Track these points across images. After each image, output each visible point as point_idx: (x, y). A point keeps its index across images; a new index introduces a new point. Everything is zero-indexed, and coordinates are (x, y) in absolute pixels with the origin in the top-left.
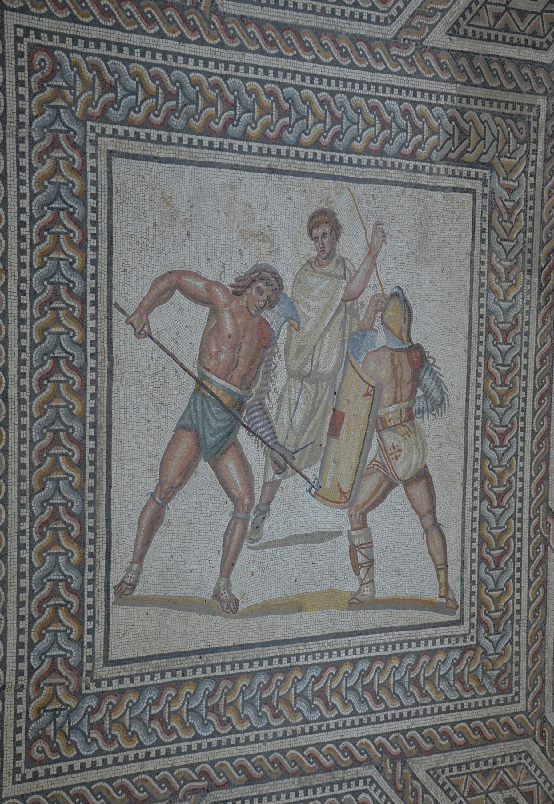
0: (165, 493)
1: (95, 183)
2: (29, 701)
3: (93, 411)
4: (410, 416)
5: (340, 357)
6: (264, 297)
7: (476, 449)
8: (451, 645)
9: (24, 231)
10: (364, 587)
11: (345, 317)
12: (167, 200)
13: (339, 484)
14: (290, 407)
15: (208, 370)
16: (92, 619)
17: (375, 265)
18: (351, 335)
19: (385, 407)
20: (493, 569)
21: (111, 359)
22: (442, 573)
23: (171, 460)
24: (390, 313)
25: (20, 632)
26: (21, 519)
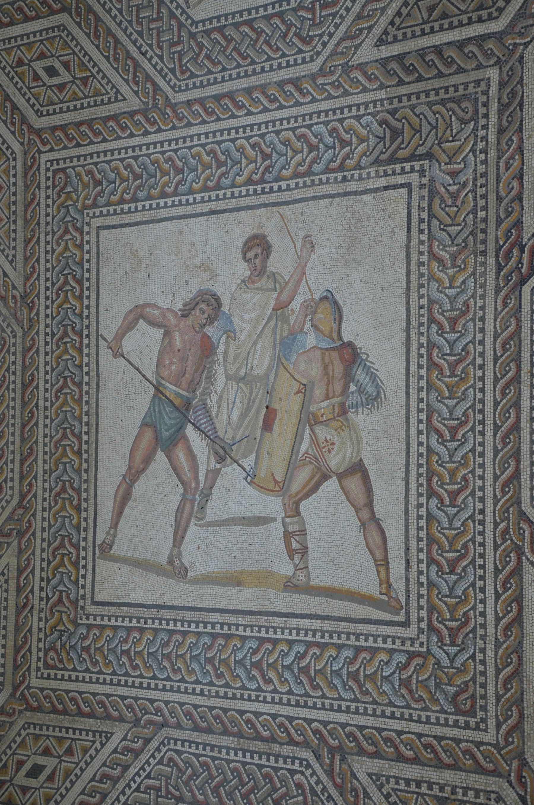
1: (88, 252)
2: (47, 621)
4: (344, 411)
5: (272, 359)
6: (206, 316)
7: (420, 444)
8: (395, 647)
10: (298, 572)
11: (276, 325)
12: (134, 253)
13: (273, 474)
14: (228, 406)
15: (163, 378)
16: (84, 567)
17: (305, 274)
18: (282, 339)
19: (317, 403)
20: (447, 574)
21: (98, 375)
22: (382, 569)
24: (319, 316)
25: (42, 569)
26: (45, 490)
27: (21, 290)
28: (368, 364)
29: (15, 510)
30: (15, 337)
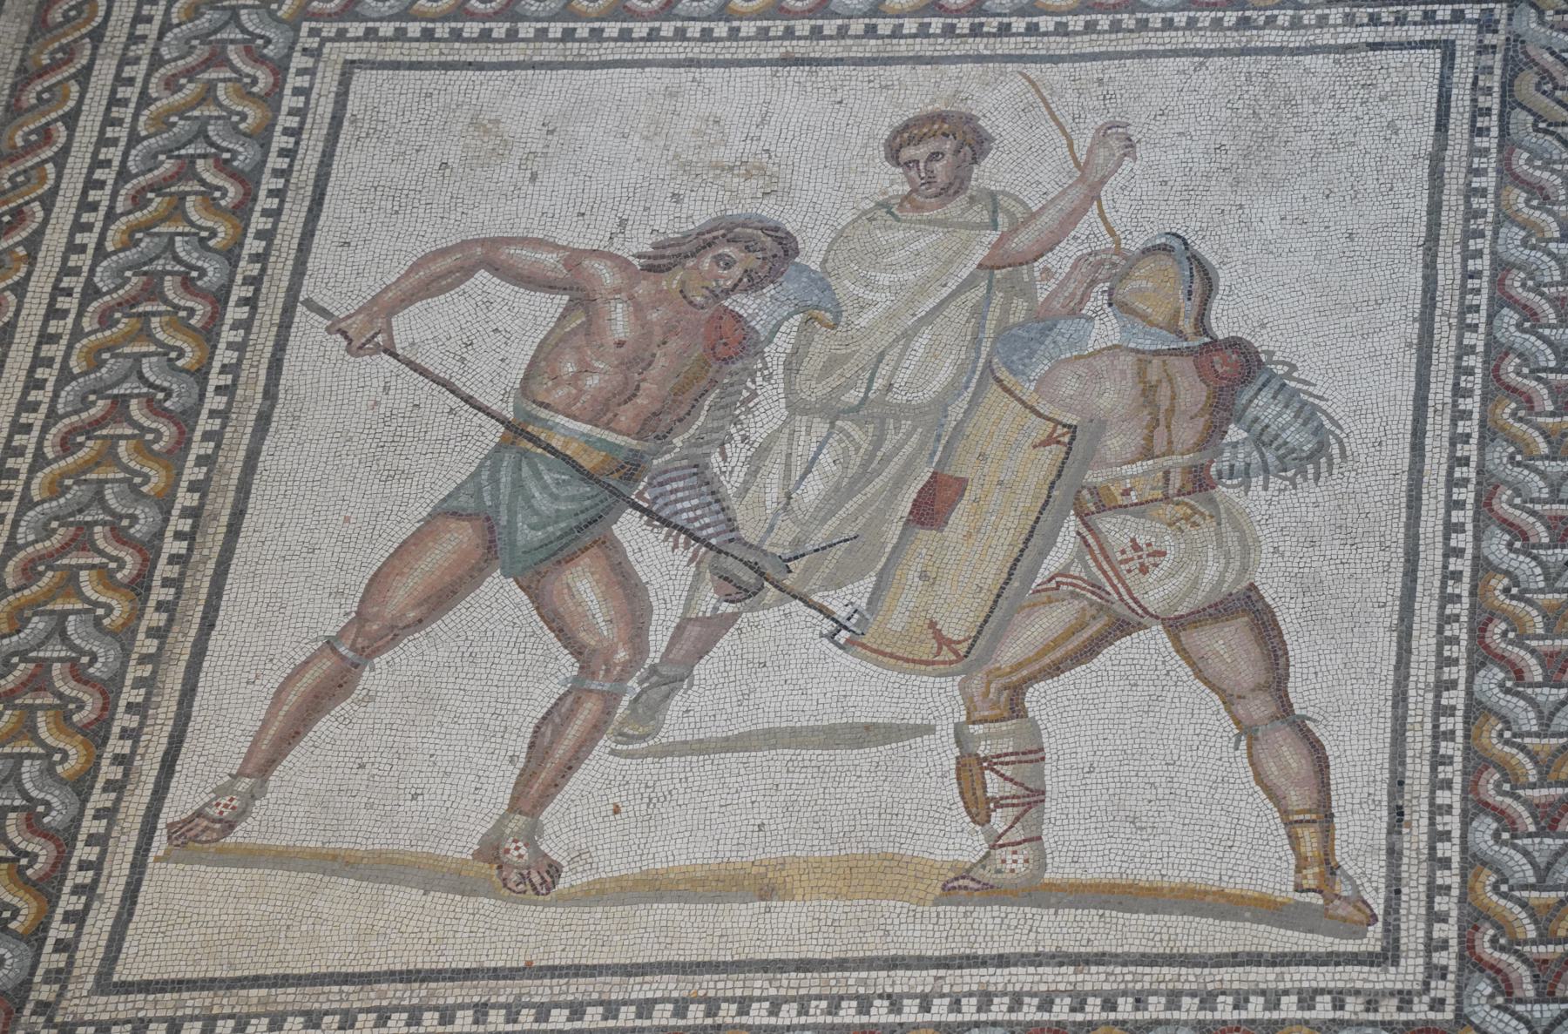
0: (369, 635)
4: (1200, 481)
20: (1530, 835)
23: (401, 574)
28: (1293, 384)
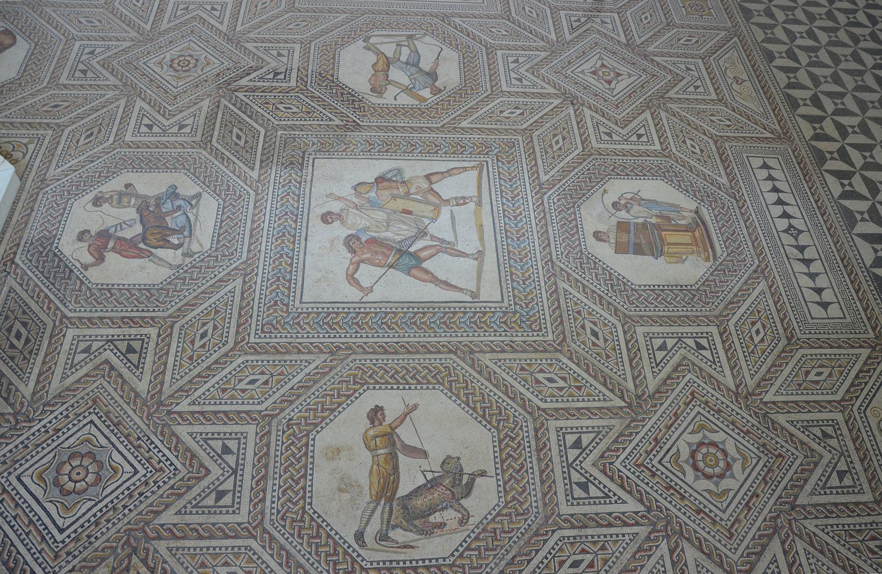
2: (517, 331)
3: (402, 309)
4: (404, 182)
9: (332, 336)
12: (319, 280)
16: (485, 308)
25: (490, 335)
26: (446, 336)
27: (327, 355)
29: (459, 357)
30: (355, 360)
